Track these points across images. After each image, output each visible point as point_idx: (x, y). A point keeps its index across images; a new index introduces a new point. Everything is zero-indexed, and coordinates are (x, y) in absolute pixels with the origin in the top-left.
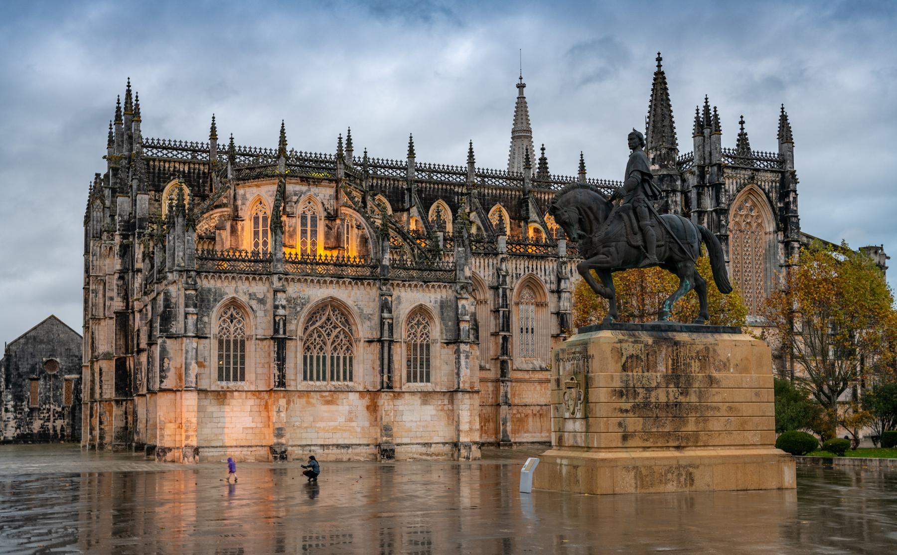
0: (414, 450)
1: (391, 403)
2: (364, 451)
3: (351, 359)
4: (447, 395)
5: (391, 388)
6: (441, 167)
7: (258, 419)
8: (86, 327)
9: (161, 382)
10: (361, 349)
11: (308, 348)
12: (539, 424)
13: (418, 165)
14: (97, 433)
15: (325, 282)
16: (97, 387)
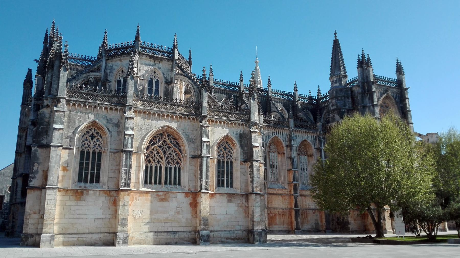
0: (222, 236)
2: (187, 236)
3: (180, 169)
4: (244, 196)
6: (226, 82)
11: (149, 161)
12: (282, 220)
13: (215, 80)
15: (163, 115)
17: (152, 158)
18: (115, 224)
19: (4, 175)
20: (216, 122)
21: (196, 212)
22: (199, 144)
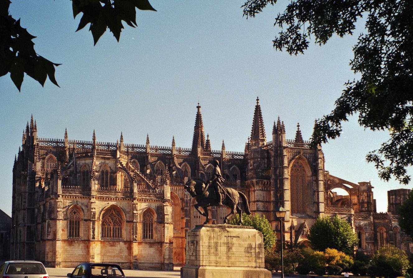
1: (137, 247)
4: (160, 244)
5: (137, 241)
9: (48, 237)
10: (125, 225)
17: (105, 223)
20: (143, 200)
22: (132, 214)
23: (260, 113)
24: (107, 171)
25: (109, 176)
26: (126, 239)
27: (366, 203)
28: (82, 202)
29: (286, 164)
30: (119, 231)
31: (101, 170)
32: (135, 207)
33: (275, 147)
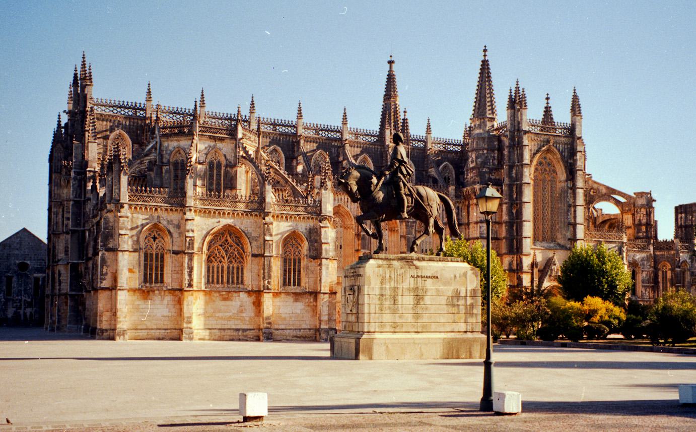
5: (270, 290)
7: (173, 310)
8: (49, 238)
9: (101, 282)
13: (305, 124)
14: (56, 318)
15: (224, 213)
16: (57, 284)
17: (214, 257)
18: (181, 321)
19: (10, 247)
20: (282, 217)
21: (260, 310)
22: (262, 242)
23: (489, 73)
24: (219, 162)
25: (222, 172)
26: (250, 286)
27: (644, 225)
28: (169, 219)
29: (527, 160)
30: (238, 273)
31: (208, 161)
32: (269, 230)
33: (510, 132)
